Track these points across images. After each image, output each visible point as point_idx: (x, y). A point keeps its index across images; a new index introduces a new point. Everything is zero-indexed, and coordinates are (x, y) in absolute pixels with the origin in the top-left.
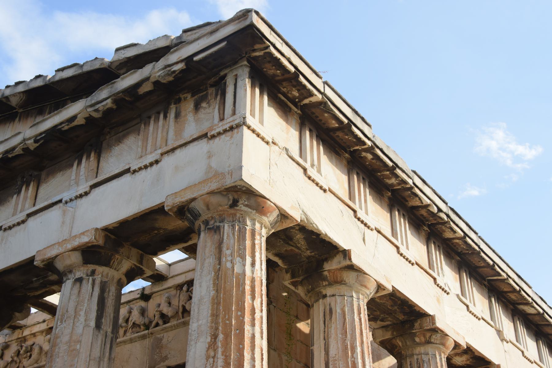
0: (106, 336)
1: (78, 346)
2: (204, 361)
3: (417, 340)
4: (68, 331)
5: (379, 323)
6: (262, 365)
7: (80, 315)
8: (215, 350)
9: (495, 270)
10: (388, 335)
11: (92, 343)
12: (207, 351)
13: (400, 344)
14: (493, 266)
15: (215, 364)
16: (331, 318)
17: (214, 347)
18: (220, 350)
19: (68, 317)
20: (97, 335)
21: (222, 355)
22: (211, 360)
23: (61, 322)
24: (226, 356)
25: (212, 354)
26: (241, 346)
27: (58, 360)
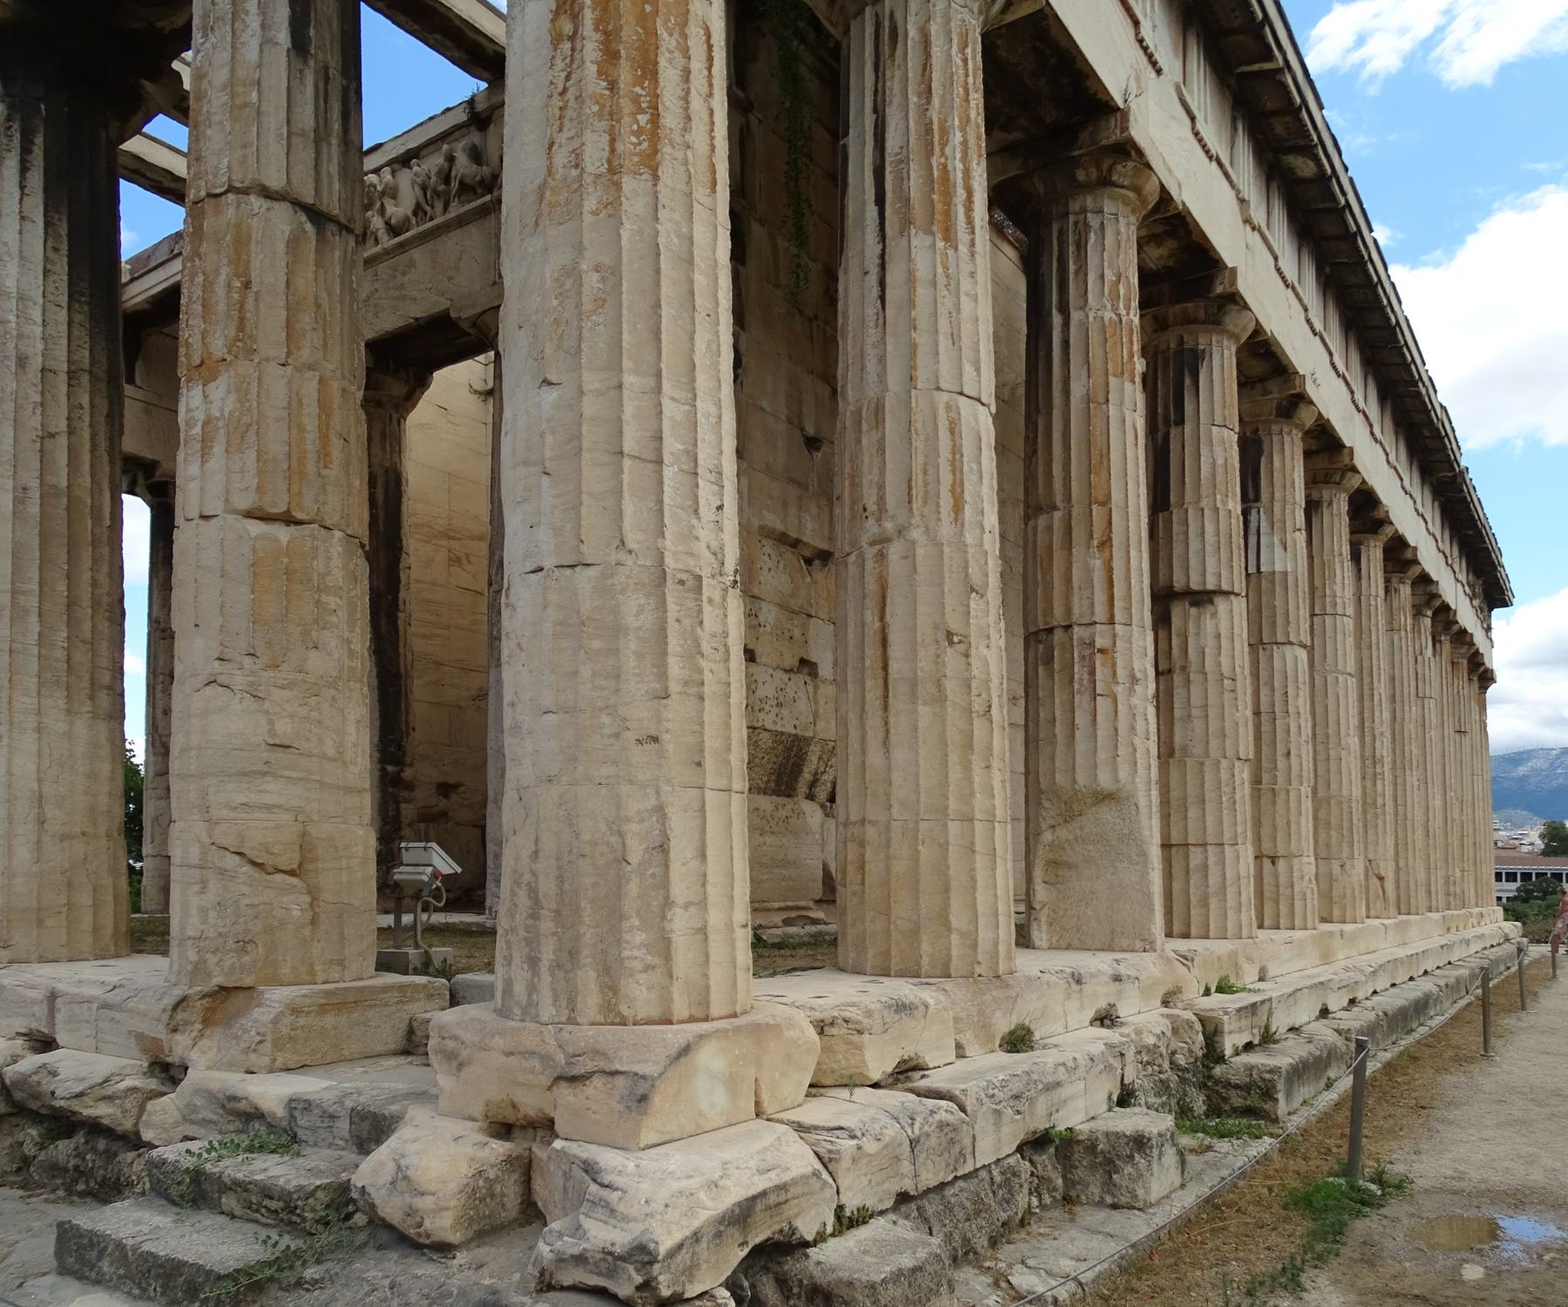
0: (327, 79)
1: (254, 95)
2: (547, 51)
3: (1081, 175)
4: (223, 56)
5: (999, 135)
6: (710, 76)
7: (247, 13)
8: (576, 18)
9: (1263, 38)
10: (1014, 169)
11: (289, 88)
12: (553, 21)
13: (1041, 189)
14: (1262, 25)
15: (577, 55)
16: (892, 55)
17: (572, 8)
18: (589, 17)
19: (217, 19)
20: (301, 71)
21: (596, 29)
22: (568, 45)
23: (205, 35)
24: (606, 33)
25: (568, 28)
26: (648, 8)
27: (209, 132)
